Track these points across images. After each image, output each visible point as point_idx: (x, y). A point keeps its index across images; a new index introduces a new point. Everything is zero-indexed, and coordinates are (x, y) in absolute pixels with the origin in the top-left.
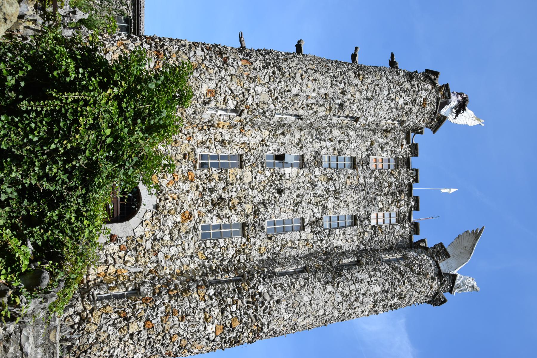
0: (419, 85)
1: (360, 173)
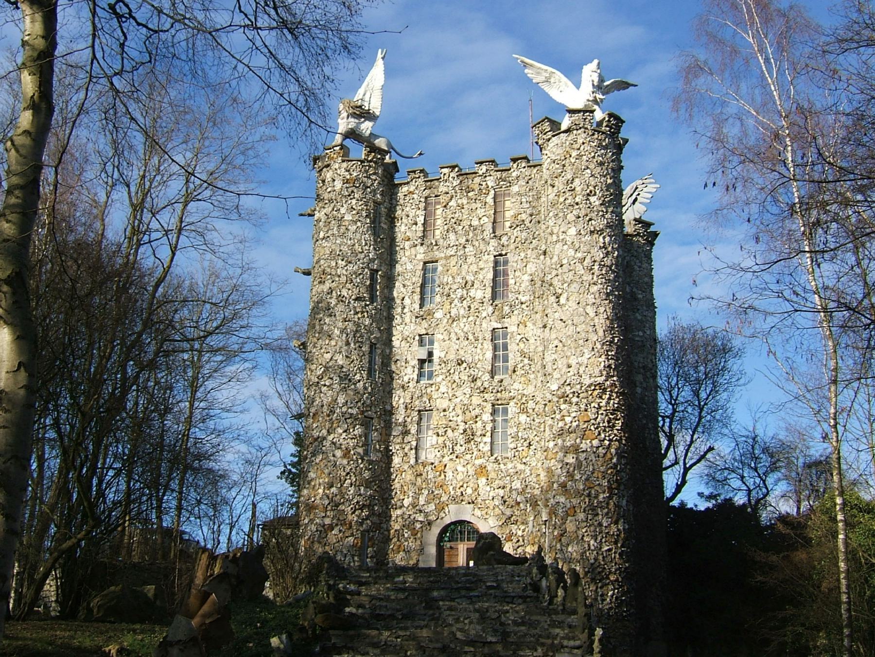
1: (443, 255)
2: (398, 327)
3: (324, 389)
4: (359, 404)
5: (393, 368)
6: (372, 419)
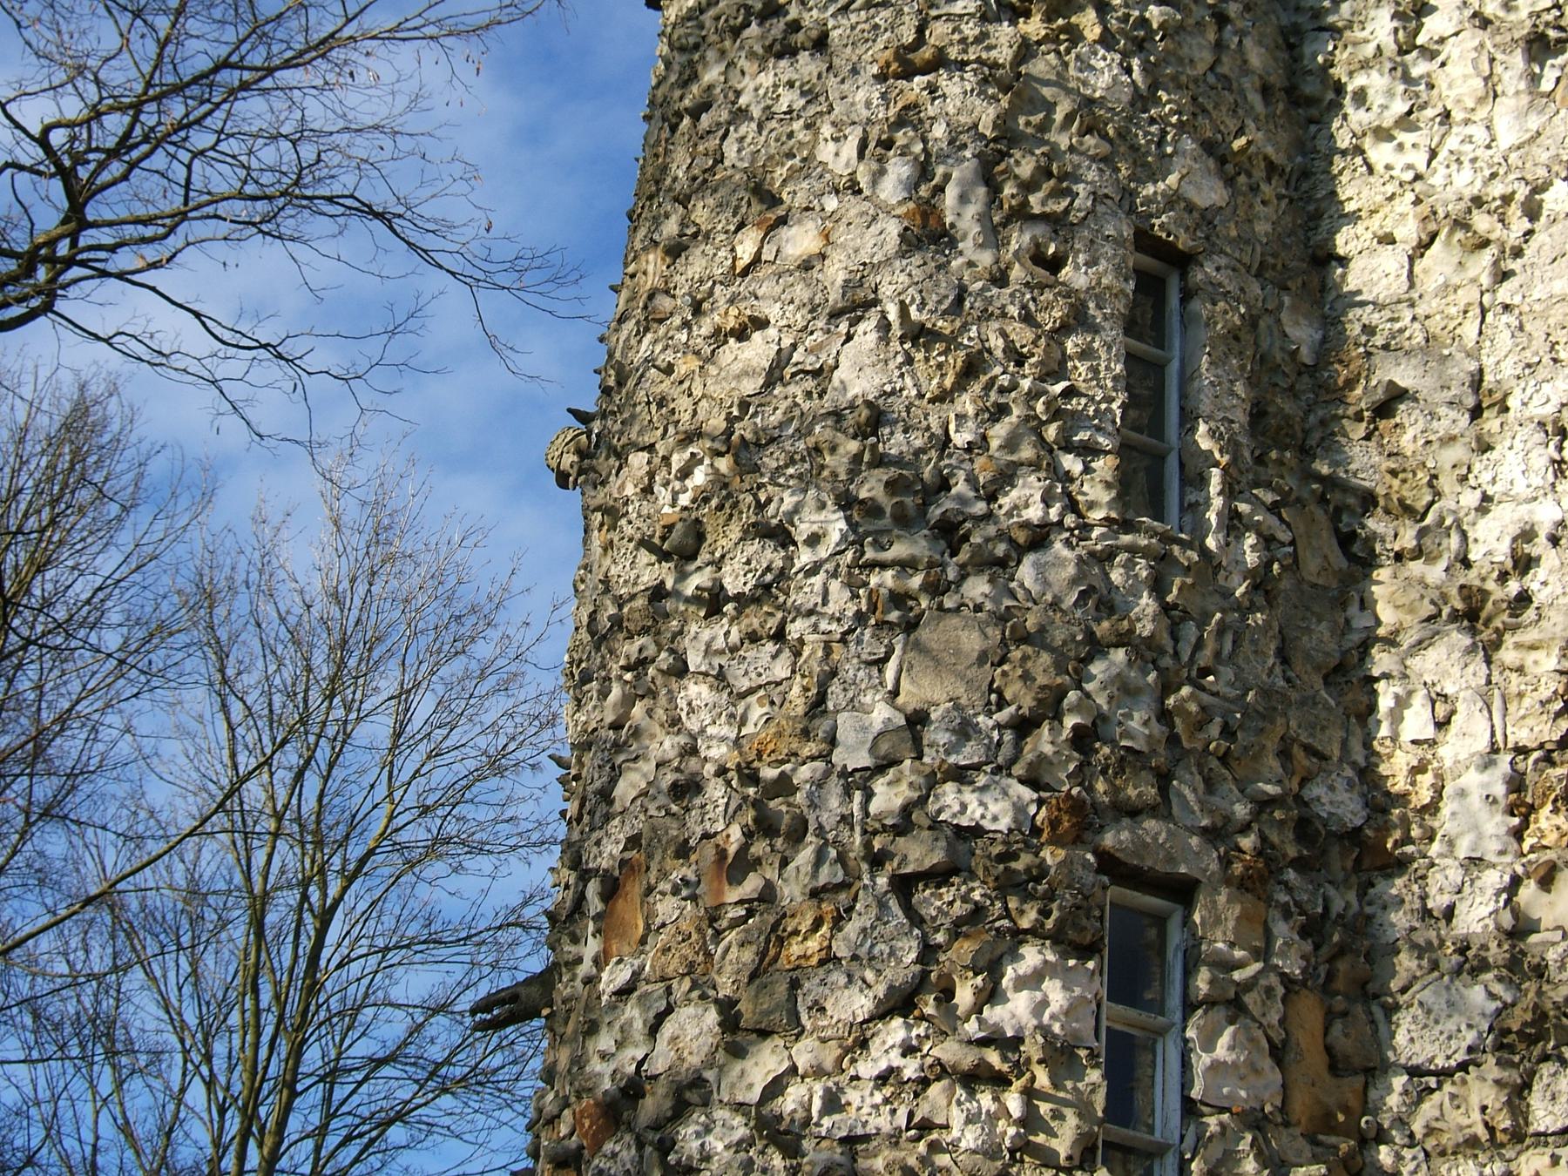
2: (1380, 154)
3: (703, 638)
4: (1044, 742)
5: (1364, 462)
6: (1183, 891)
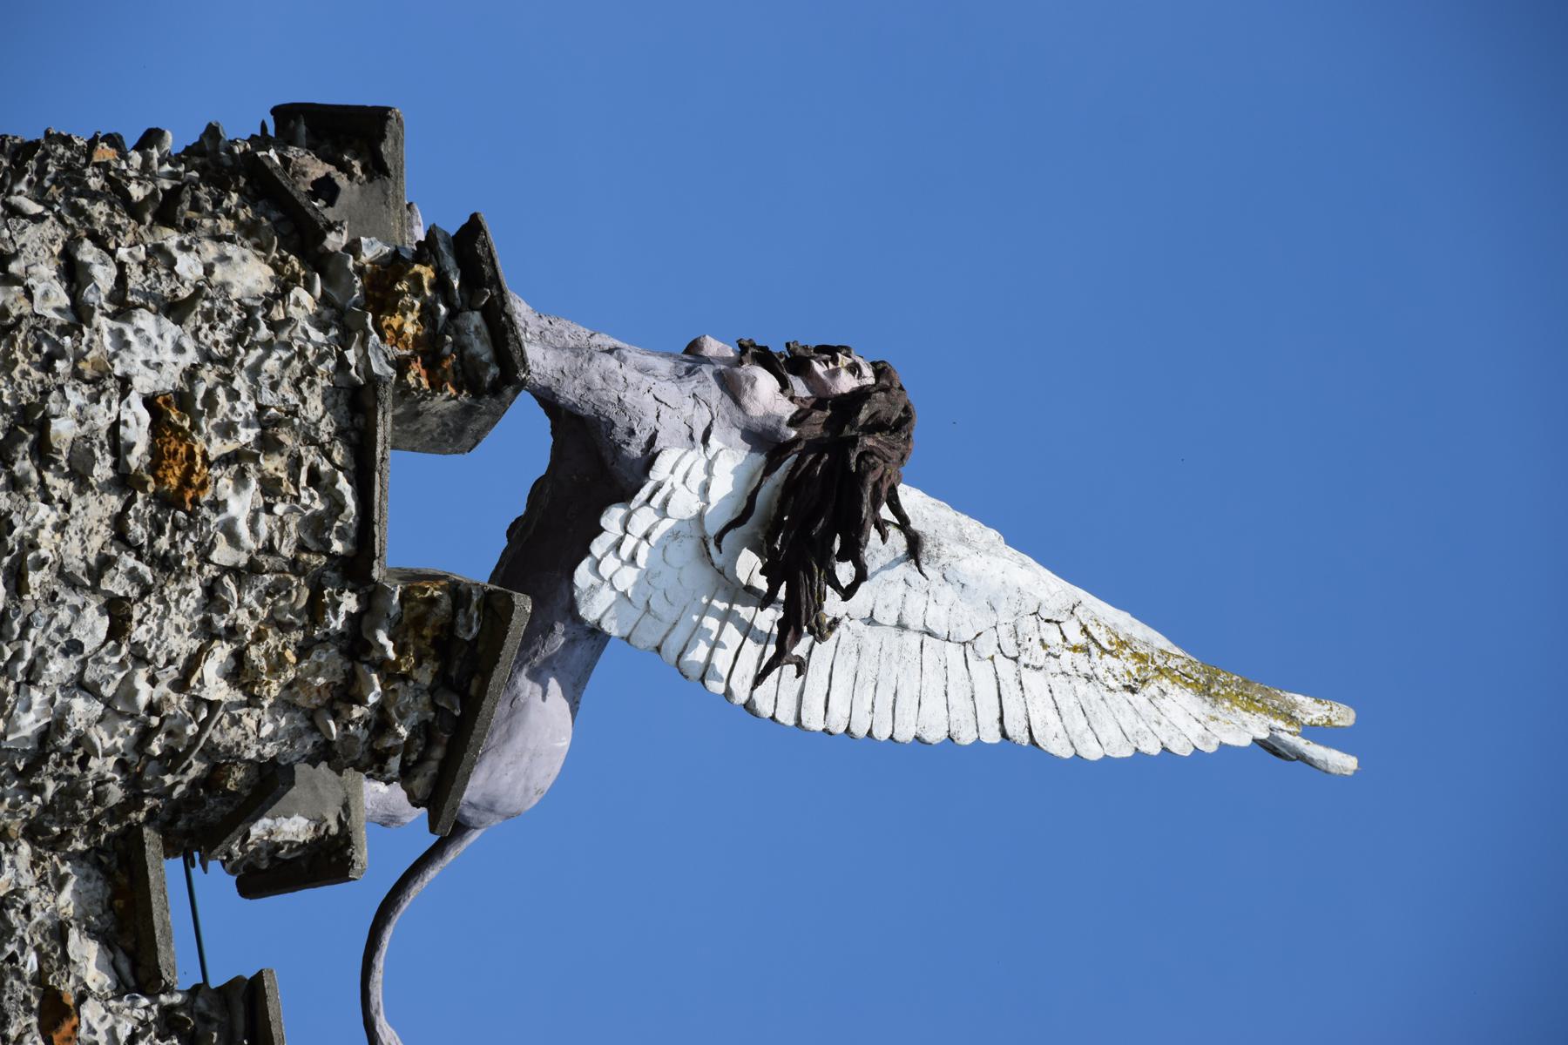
0: (88, 252)
